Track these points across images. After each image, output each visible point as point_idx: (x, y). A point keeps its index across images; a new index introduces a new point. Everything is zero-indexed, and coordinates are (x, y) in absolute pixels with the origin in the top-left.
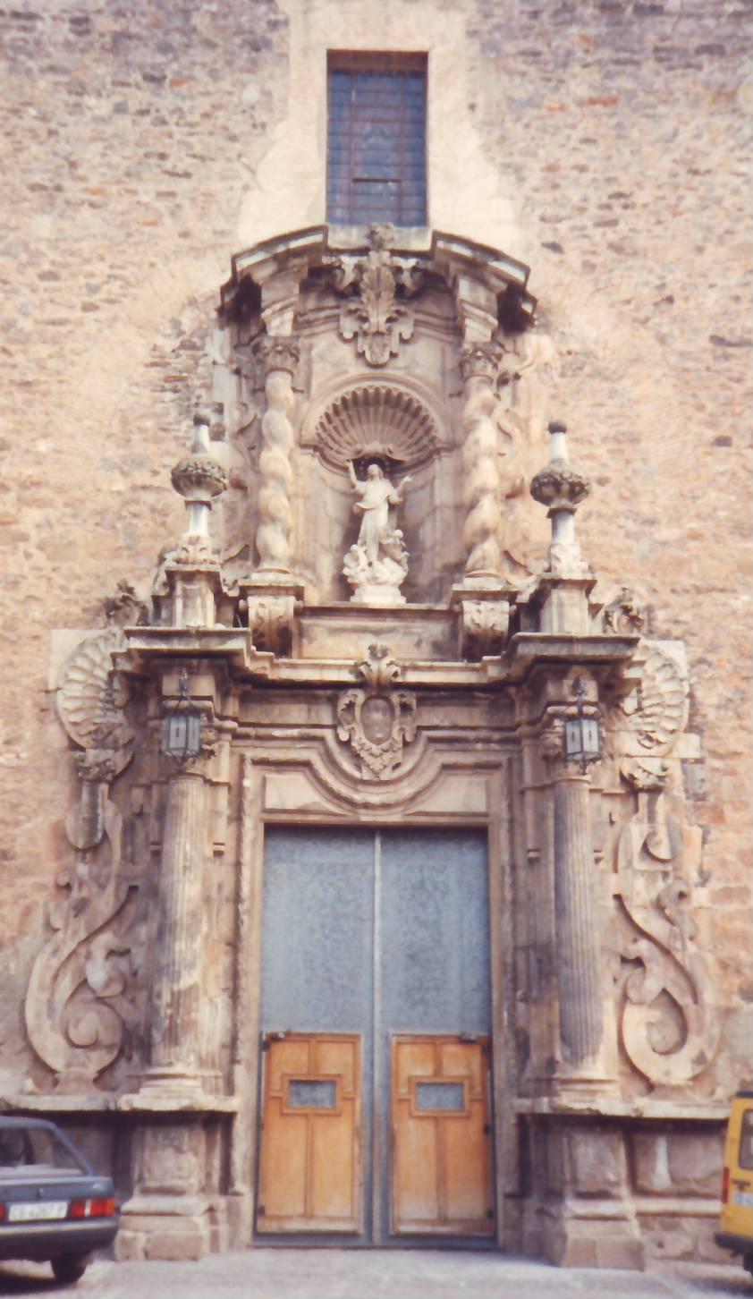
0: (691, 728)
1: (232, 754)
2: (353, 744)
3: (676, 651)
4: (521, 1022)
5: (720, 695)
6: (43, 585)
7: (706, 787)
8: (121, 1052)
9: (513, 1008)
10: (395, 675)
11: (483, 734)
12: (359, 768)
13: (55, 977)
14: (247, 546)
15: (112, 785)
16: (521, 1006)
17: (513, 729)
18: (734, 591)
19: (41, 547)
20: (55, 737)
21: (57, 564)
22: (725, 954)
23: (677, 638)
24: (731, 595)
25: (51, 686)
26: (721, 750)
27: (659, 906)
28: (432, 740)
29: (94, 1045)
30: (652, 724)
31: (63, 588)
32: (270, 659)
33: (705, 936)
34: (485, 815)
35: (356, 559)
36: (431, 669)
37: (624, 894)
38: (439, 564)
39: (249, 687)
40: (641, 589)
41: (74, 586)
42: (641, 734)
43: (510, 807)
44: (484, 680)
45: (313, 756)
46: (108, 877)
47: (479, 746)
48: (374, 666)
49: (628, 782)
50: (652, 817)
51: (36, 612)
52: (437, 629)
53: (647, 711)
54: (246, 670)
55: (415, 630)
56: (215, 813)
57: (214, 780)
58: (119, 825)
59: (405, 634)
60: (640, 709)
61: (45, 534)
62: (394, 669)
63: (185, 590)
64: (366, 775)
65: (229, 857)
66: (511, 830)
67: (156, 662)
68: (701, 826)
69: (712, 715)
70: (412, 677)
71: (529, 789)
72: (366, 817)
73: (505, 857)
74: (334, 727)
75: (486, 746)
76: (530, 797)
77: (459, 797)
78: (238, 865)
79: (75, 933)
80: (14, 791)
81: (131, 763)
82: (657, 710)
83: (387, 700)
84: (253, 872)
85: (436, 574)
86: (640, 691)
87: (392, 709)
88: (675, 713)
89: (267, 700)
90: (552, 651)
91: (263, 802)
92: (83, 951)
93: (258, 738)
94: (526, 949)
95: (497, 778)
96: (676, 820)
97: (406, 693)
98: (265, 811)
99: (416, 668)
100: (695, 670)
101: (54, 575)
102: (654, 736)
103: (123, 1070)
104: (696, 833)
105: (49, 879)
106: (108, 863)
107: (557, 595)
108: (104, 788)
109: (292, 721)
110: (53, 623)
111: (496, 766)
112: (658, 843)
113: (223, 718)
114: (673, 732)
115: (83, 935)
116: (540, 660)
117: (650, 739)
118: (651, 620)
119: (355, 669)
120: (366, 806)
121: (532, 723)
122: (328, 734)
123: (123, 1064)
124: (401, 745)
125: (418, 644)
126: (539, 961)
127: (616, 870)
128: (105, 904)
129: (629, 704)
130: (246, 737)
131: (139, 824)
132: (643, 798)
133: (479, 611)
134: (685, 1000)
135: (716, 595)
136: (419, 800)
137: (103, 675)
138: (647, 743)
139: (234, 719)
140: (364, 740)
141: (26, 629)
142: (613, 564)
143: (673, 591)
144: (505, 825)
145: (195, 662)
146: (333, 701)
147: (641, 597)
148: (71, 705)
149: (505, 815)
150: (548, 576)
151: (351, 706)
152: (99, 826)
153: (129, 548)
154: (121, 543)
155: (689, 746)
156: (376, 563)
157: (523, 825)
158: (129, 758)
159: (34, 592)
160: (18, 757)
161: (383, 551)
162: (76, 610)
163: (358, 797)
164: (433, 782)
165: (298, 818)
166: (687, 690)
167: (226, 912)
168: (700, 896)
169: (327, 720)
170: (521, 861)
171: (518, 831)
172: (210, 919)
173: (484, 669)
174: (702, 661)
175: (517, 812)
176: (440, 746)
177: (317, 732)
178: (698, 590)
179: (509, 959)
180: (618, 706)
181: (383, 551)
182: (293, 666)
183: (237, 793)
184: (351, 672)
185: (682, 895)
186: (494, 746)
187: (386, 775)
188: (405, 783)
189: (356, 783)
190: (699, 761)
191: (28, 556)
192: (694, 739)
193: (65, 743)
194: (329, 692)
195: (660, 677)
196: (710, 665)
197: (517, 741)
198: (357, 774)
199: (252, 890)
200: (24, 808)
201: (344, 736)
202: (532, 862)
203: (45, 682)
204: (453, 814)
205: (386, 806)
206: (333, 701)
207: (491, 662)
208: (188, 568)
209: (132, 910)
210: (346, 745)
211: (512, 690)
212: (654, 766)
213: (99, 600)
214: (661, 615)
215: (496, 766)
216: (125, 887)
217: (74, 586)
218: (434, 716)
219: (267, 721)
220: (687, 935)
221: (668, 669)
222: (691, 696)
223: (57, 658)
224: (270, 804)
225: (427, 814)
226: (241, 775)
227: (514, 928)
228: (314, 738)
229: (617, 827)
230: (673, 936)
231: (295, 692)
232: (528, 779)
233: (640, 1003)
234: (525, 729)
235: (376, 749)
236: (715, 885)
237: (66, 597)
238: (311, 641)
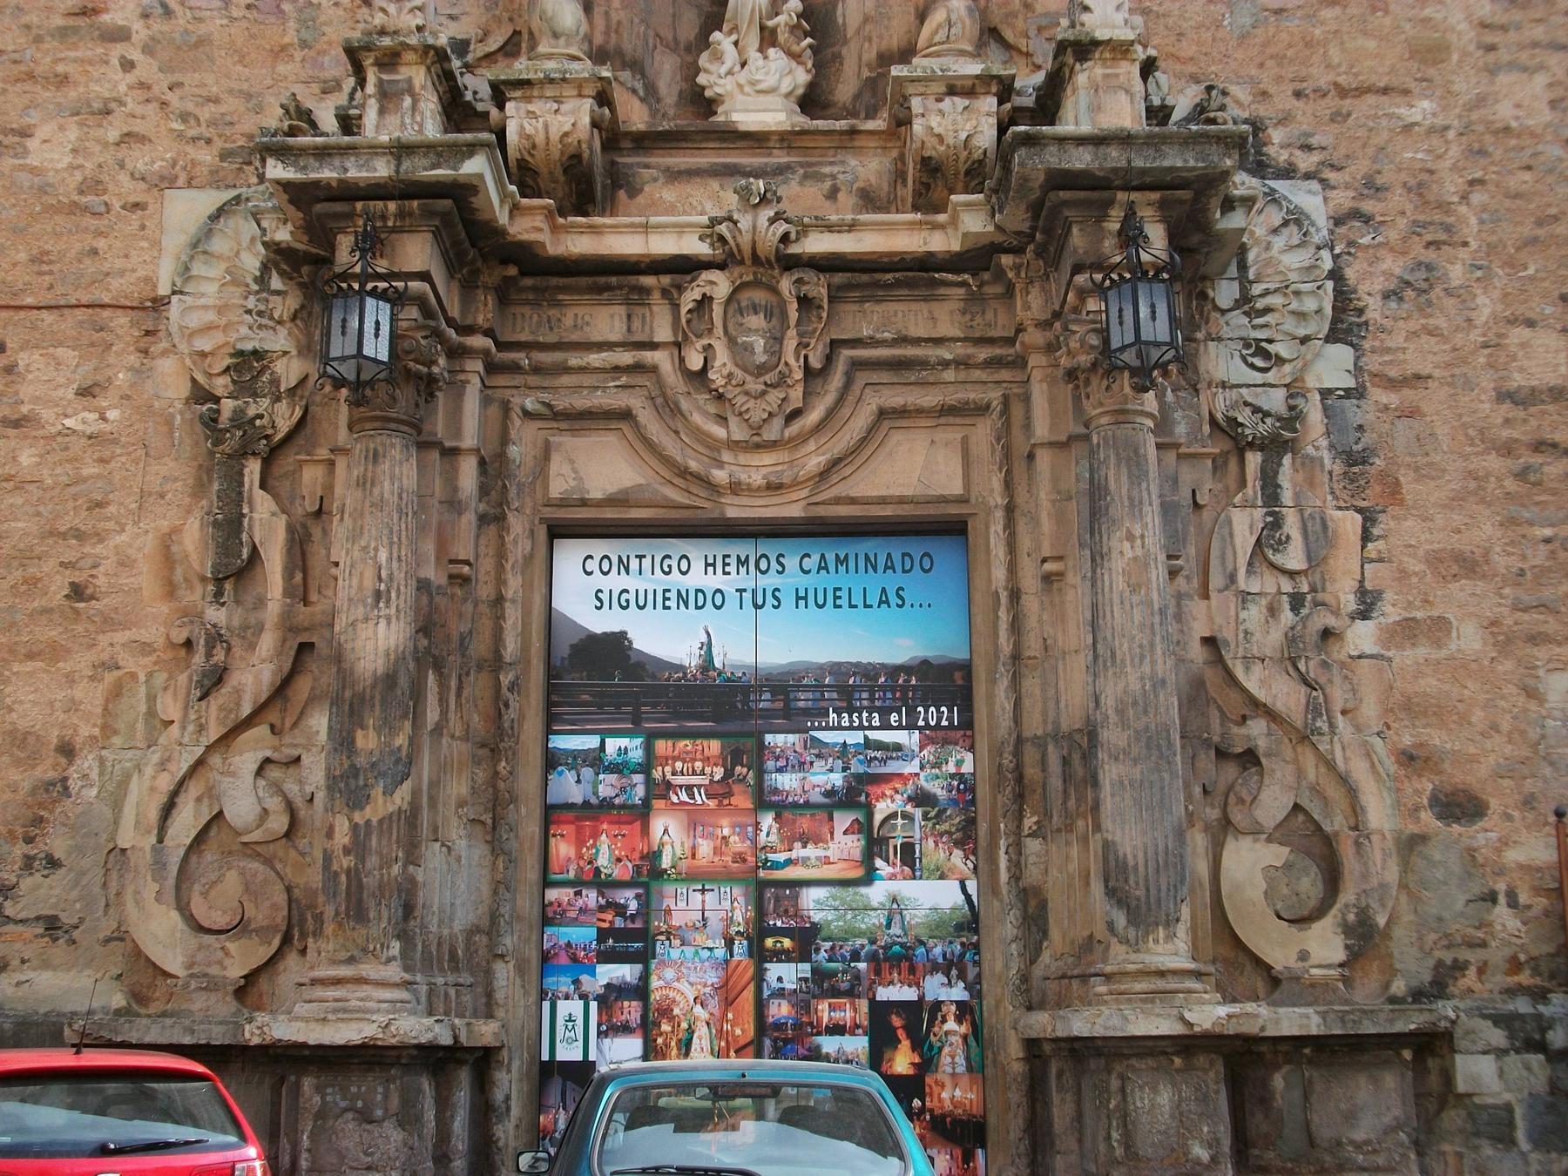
0: (1335, 335)
1: (486, 401)
2: (711, 375)
3: (1307, 198)
4: (1032, 875)
5: (1388, 275)
6: (152, 109)
7: (1368, 439)
8: (287, 940)
9: (1017, 847)
10: (785, 238)
11: (960, 350)
12: (722, 420)
13: (168, 809)
14: (516, 33)
15: (267, 463)
16: (1033, 846)
17: (1010, 341)
18: (1406, 92)
19: (148, 50)
20: (170, 381)
21: (177, 77)
22: (1407, 740)
23: (1308, 176)
24: (1398, 100)
25: (163, 290)
26: (1393, 373)
27: (1290, 658)
28: (857, 365)
29: (240, 927)
30: (1265, 326)
31: (184, 117)
32: (549, 215)
33: (1370, 710)
34: (963, 500)
35: (718, 57)
36: (852, 227)
37: (1227, 634)
38: (870, 55)
39: (512, 271)
40: (1240, 92)
41: (206, 113)
42: (1247, 346)
43: (1008, 485)
44: (956, 246)
45: (635, 402)
46: (260, 628)
47: (949, 375)
48: (745, 222)
49: (1226, 429)
50: (1271, 494)
51: (140, 159)
52: (870, 167)
53: (1260, 304)
54: (502, 232)
55: (827, 170)
56: (453, 504)
57: (448, 444)
58: (281, 535)
59: (806, 177)
60: (1244, 300)
61: (158, 26)
62: (782, 227)
63: (381, 81)
64: (738, 432)
65: (485, 591)
66: (1010, 524)
67: (320, 208)
68: (1359, 510)
69: (1374, 309)
70: (817, 244)
71: (1042, 445)
72: (736, 509)
73: (999, 574)
74: (678, 345)
75: (962, 375)
76: (1044, 459)
77: (914, 468)
78: (499, 600)
79: (201, 728)
80: (98, 476)
81: (302, 422)
82: (1275, 300)
83: (775, 291)
84: (527, 614)
85: (866, 73)
86: (1243, 267)
87: (783, 304)
88: (1310, 305)
89: (546, 298)
90: (1081, 159)
91: (546, 487)
92: (215, 760)
93: (537, 370)
94: (1040, 743)
95: (983, 433)
96: (1312, 502)
97: (809, 275)
98: (549, 504)
99: (830, 228)
100: (1342, 230)
101: (173, 98)
102: (1271, 348)
103: (293, 969)
104: (1350, 523)
105: (153, 633)
106: (261, 602)
107: (1084, 77)
108: (253, 468)
109: (596, 337)
110: (166, 182)
111: (983, 409)
112: (1282, 544)
113: (468, 330)
114: (1304, 340)
115: (214, 733)
116: (1062, 180)
117: (1266, 355)
118: (1260, 145)
119: (710, 233)
120: (736, 488)
121: (1045, 325)
122: (661, 358)
123: (292, 960)
124: (799, 375)
125: (832, 194)
126: (1066, 762)
127: (1207, 597)
128: (254, 675)
129: (1225, 293)
130: (515, 368)
131: (317, 532)
132: (1254, 460)
133: (941, 113)
134: (1336, 823)
135: (1371, 99)
136: (835, 478)
137: (251, 262)
138: (1259, 362)
139: (489, 333)
140: (730, 367)
141: (125, 187)
142: (1187, 49)
143: (1298, 94)
144: (999, 515)
145: (392, 206)
146: (671, 296)
147: (1238, 103)
148: (194, 320)
149: (999, 499)
150: (1070, 35)
151: (705, 302)
152: (244, 537)
153: (304, 44)
154: (291, 37)
155: (1332, 367)
156: (753, 55)
157: (1035, 521)
158: (298, 413)
159: (138, 127)
160: (103, 418)
161: (768, 38)
162: (206, 157)
163: (720, 476)
164: (863, 442)
165: (610, 514)
166: (1328, 264)
167: (478, 685)
168: (1362, 637)
169: (663, 333)
170: (1029, 580)
171: (1022, 526)
172: (443, 701)
173: (954, 222)
174: (1355, 214)
175: (1021, 498)
176: (875, 377)
177: (649, 356)
178: (1343, 92)
179: (1007, 760)
180: (1203, 296)
181: (768, 38)
182: (594, 230)
183: (494, 468)
184: (701, 239)
185: (1327, 634)
186: (977, 374)
187: (772, 432)
188: (811, 446)
189: (713, 447)
190: (1356, 393)
191: (128, 65)
192: (1341, 354)
193: (185, 390)
194: (666, 280)
195: (1279, 242)
196: (1367, 219)
197: (1020, 363)
198: (720, 432)
199: (525, 647)
200: (112, 509)
201: (695, 362)
202: (1048, 579)
203: (150, 281)
204: (901, 500)
205: (773, 487)
206: (671, 296)
207: (968, 204)
208: (386, 41)
209: (303, 686)
210: (700, 377)
211: (1006, 260)
212: (1275, 401)
213: (251, 137)
214: (1276, 135)
215: (983, 409)
216: (293, 645)
217: (206, 113)
218: (869, 321)
219: (551, 338)
220: (1337, 706)
221: (1293, 228)
222: (1336, 275)
223: (175, 242)
224: (557, 489)
225: (853, 501)
226: (505, 440)
227: (1018, 705)
228: (638, 368)
229: (1207, 515)
230: (1313, 709)
231: (602, 280)
232: (1041, 430)
233: (1255, 831)
234: (1034, 336)
235: (755, 386)
236: (1390, 611)
237: (192, 133)
238: (634, 192)
